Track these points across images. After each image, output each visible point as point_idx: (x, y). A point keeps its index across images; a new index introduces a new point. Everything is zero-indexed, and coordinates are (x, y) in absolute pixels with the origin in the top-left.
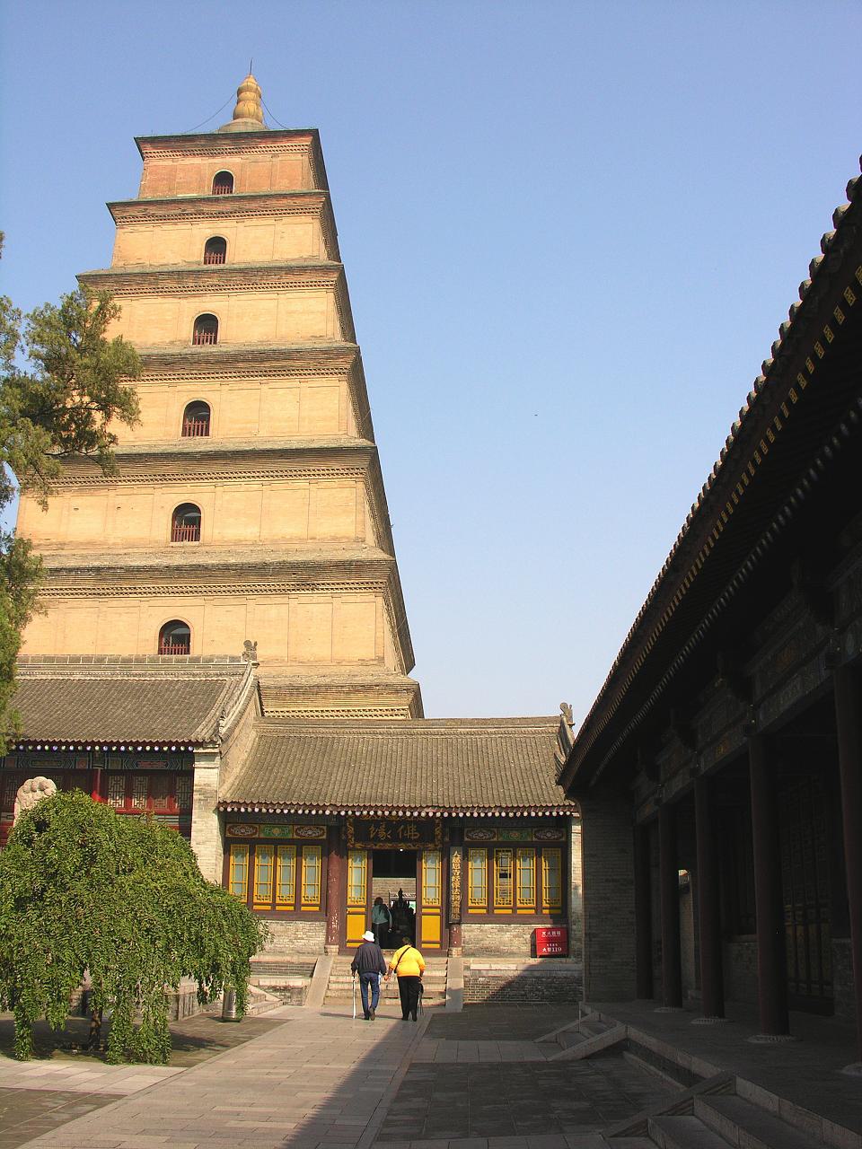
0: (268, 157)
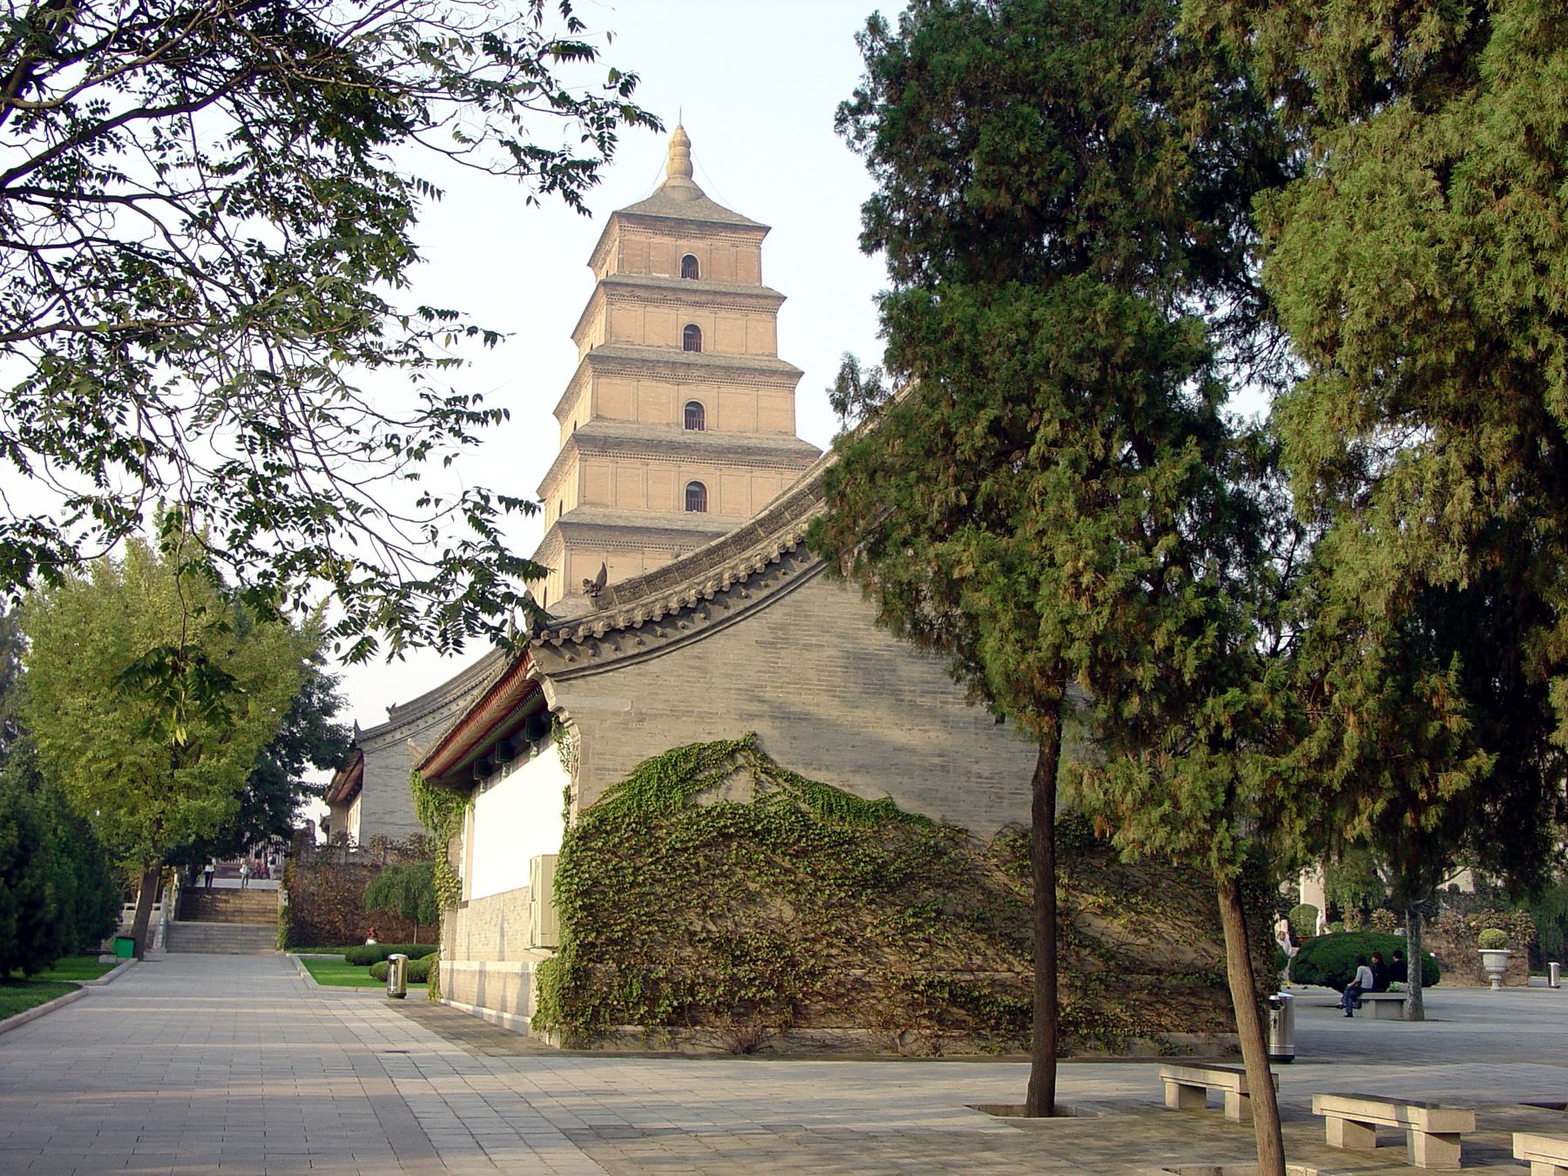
0: (727, 245)
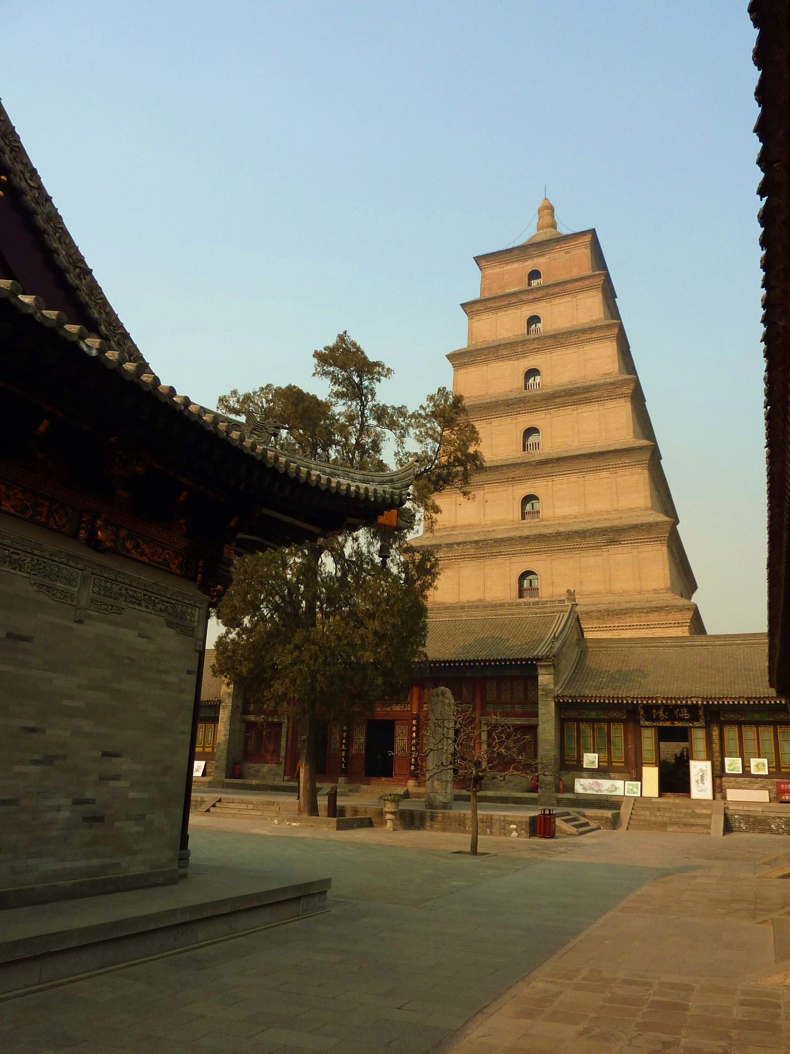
0: (563, 253)
